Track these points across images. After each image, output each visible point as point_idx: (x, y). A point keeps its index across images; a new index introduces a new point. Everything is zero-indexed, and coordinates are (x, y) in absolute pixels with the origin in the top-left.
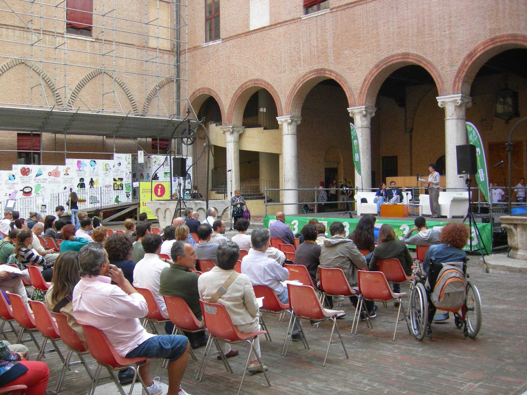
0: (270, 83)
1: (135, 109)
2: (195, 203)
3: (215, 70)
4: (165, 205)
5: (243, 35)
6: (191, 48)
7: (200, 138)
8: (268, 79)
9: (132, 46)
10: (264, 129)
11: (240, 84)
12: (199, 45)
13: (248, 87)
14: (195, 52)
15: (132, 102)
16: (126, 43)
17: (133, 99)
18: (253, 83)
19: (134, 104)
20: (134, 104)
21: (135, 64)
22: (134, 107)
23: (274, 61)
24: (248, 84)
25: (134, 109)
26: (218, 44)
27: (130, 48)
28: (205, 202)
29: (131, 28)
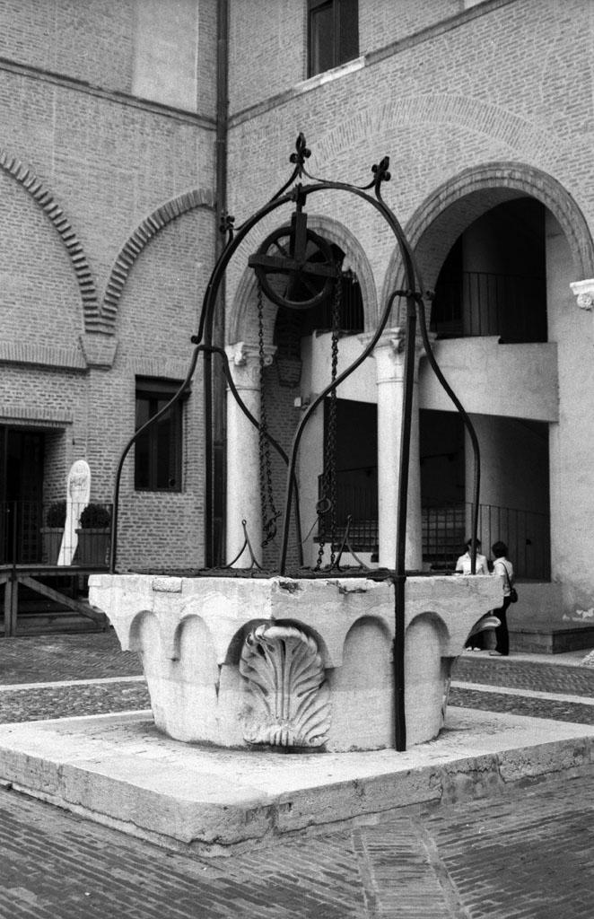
0: (544, 169)
1: (86, 280)
2: (343, 590)
3: (339, 158)
4: (176, 601)
5: (443, 29)
6: (262, 104)
7: (283, 383)
8: (535, 159)
9: (80, 87)
10: (501, 342)
11: (429, 191)
12: (287, 89)
13: (457, 196)
14: (276, 112)
15: (75, 258)
16: (63, 72)
17: (78, 248)
18: (479, 177)
19: (83, 264)
20: (83, 264)
21: (87, 141)
22: (80, 273)
23: (561, 91)
24: (461, 184)
25: (82, 281)
26: (354, 73)
27: (72, 93)
28: (387, 588)
29: (78, 32)
